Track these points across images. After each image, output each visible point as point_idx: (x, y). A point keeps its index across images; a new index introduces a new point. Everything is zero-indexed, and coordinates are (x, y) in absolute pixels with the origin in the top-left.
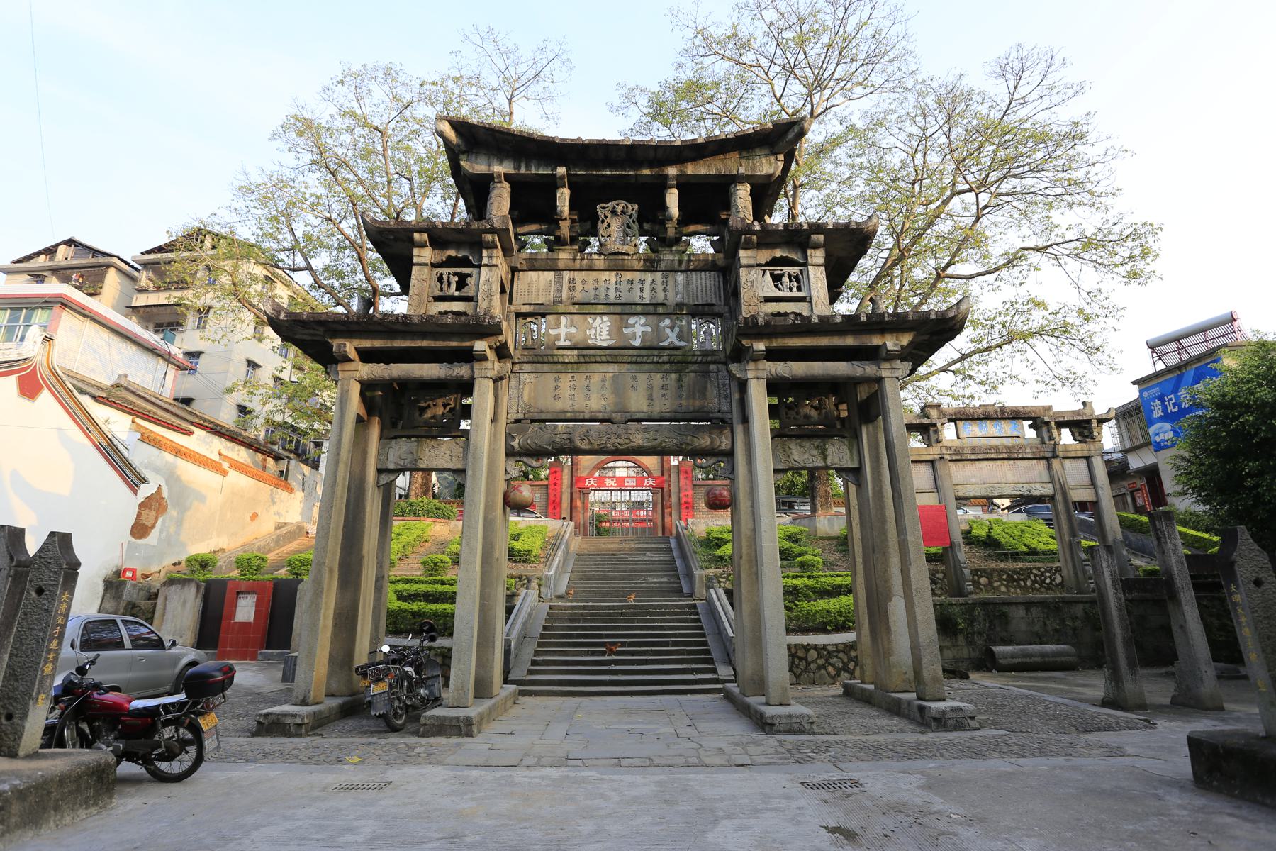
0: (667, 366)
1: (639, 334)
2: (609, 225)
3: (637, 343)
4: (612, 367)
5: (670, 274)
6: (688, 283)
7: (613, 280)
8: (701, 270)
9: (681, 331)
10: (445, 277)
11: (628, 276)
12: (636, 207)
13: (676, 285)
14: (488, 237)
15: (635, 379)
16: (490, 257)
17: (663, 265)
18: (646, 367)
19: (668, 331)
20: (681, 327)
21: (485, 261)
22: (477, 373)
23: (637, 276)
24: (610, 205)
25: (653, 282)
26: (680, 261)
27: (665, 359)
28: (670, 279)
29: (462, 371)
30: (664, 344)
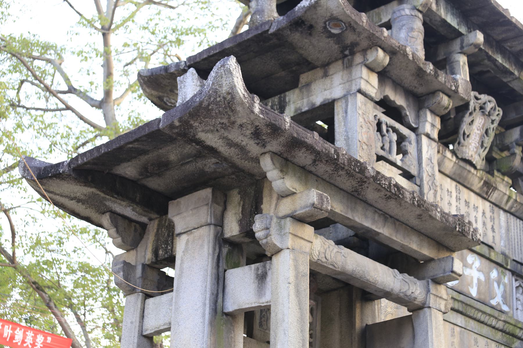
0: (499, 336)
1: (475, 281)
2: (472, 121)
3: (474, 292)
4: (460, 320)
5: (496, 209)
6: (508, 230)
7: (454, 194)
8: (518, 217)
9: (505, 291)
10: (384, 128)
11: (466, 194)
12: (501, 113)
13: (500, 227)
14: (445, 100)
15: (476, 342)
16: (433, 126)
17: (494, 196)
18: (485, 330)
19: (496, 285)
20: (505, 285)
21: (428, 128)
22: (432, 301)
23: (474, 199)
24: (484, 98)
25: (484, 213)
26: (509, 197)
27: (500, 325)
28: (495, 215)
29: (415, 288)
30: (493, 302)
